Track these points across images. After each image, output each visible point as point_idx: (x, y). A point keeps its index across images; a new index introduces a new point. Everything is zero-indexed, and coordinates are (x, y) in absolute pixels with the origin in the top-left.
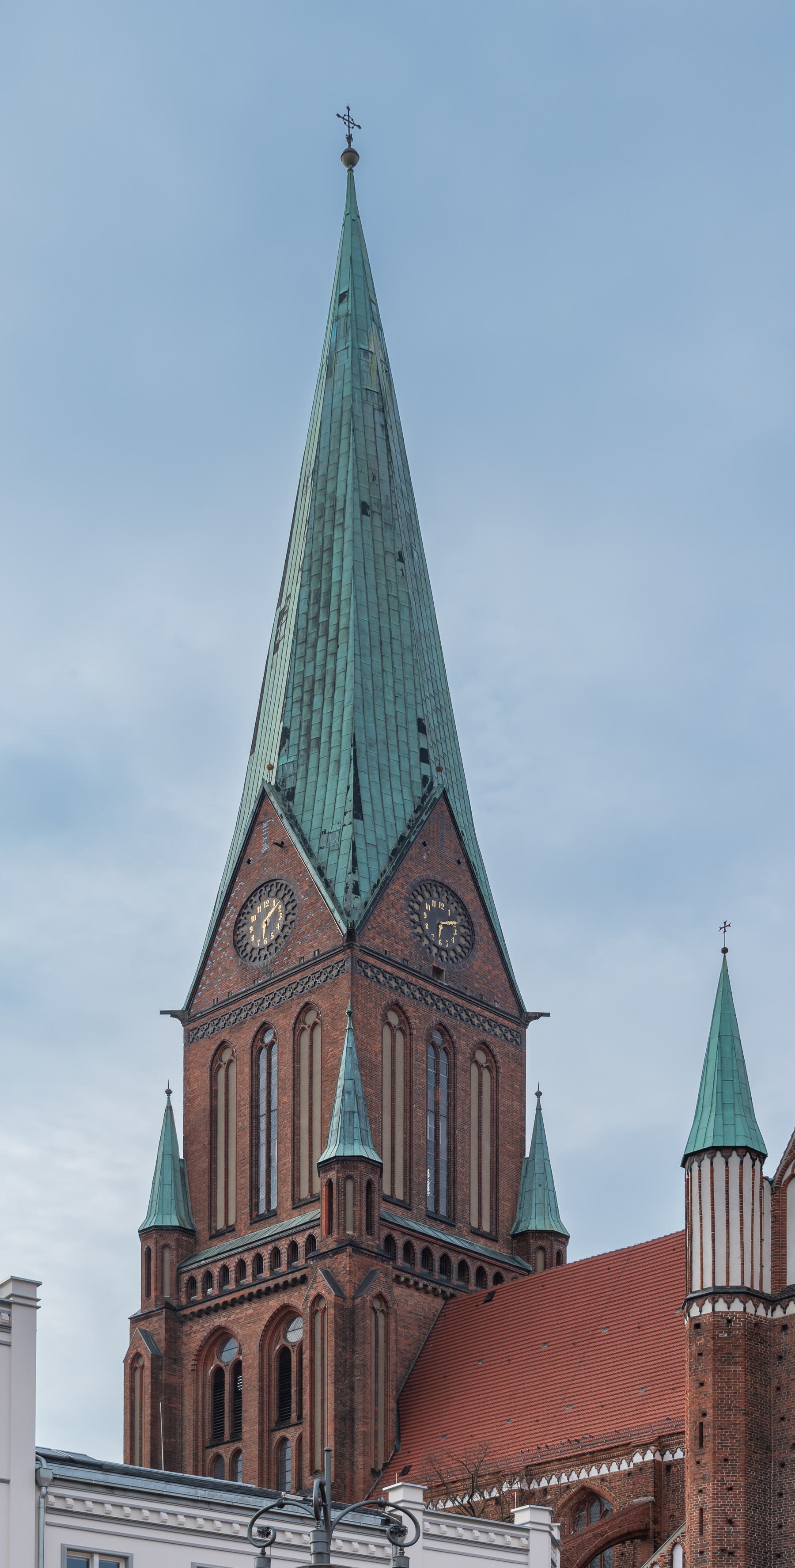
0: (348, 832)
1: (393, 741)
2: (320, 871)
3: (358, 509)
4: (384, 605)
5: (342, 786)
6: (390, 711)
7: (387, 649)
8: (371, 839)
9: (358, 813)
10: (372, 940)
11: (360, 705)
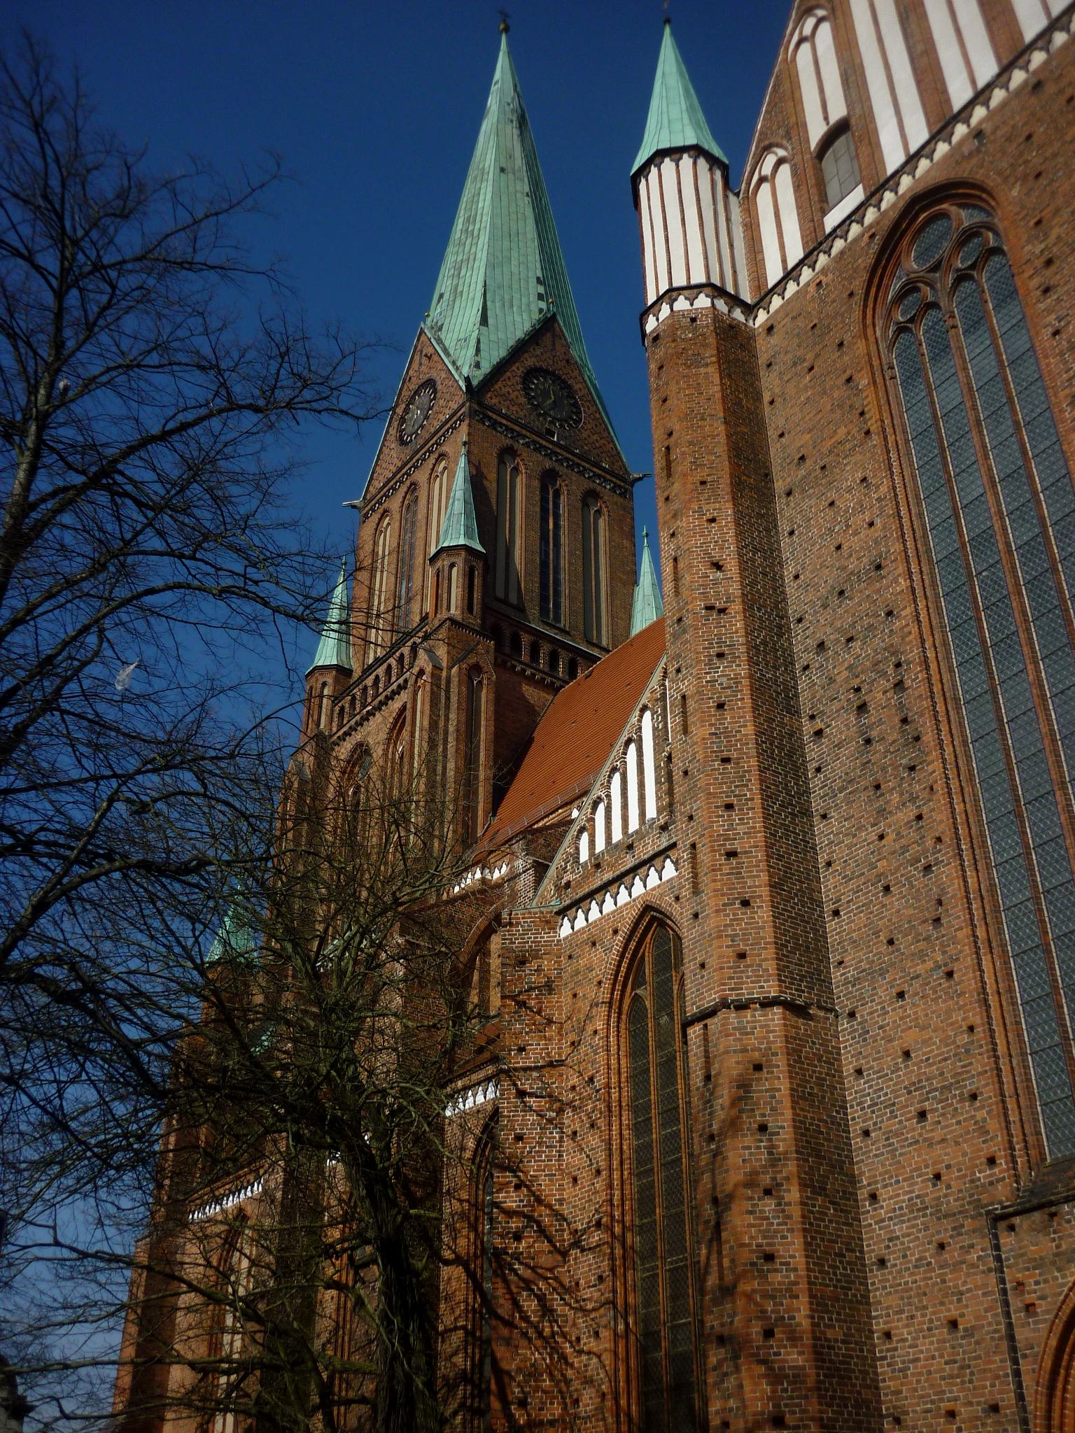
0: (475, 335)
1: (515, 286)
2: (454, 363)
3: (498, 170)
4: (513, 216)
5: (475, 311)
6: (515, 270)
7: (513, 237)
8: (493, 337)
9: (484, 321)
10: (491, 399)
11: (491, 265)
